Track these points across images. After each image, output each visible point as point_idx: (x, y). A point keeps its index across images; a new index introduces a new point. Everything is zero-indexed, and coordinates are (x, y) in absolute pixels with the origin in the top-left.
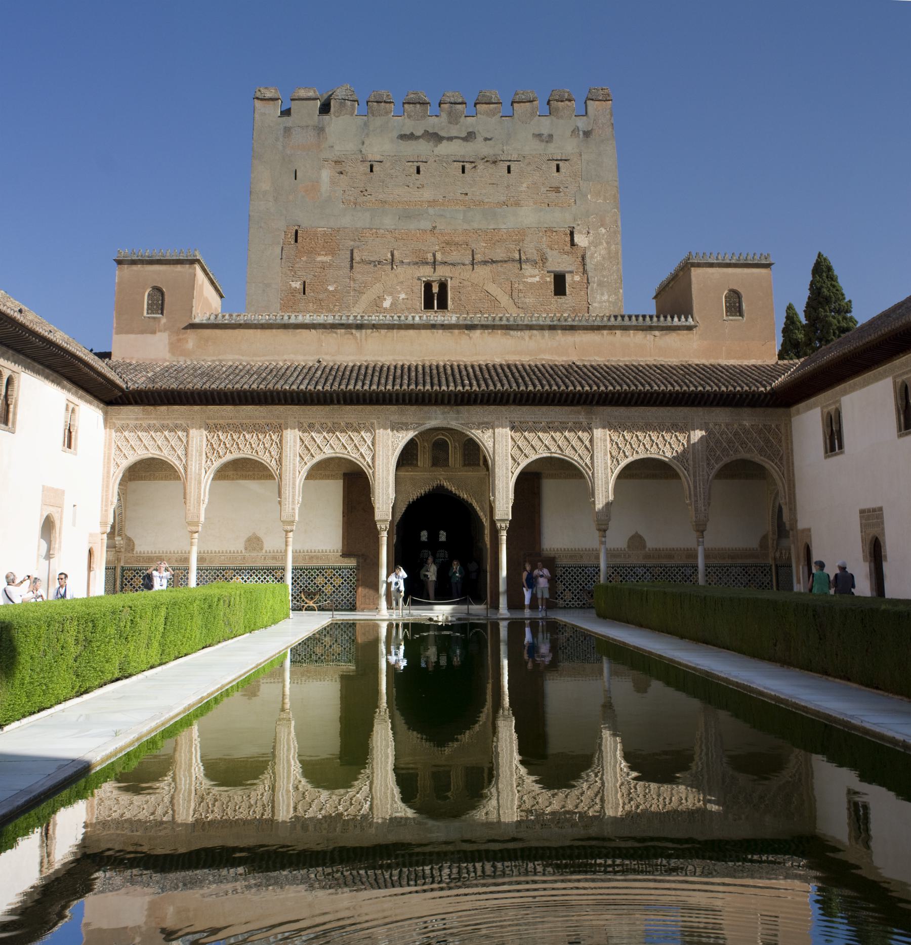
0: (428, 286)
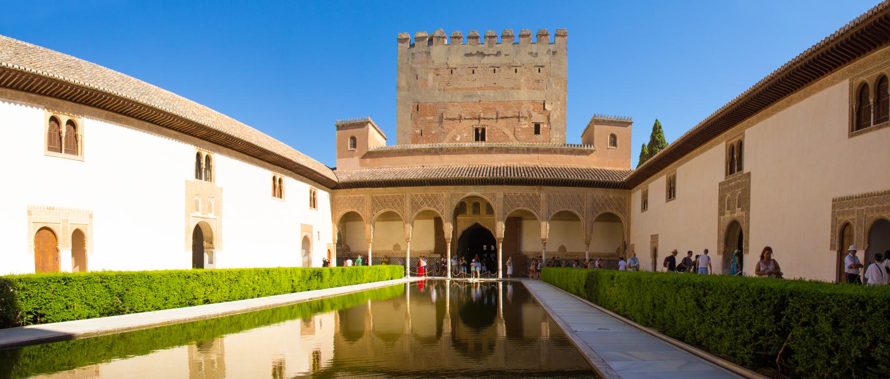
0: (477, 130)
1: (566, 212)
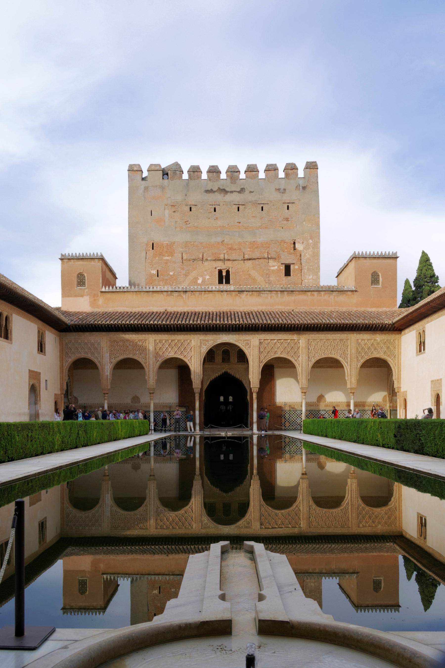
1: (326, 359)
